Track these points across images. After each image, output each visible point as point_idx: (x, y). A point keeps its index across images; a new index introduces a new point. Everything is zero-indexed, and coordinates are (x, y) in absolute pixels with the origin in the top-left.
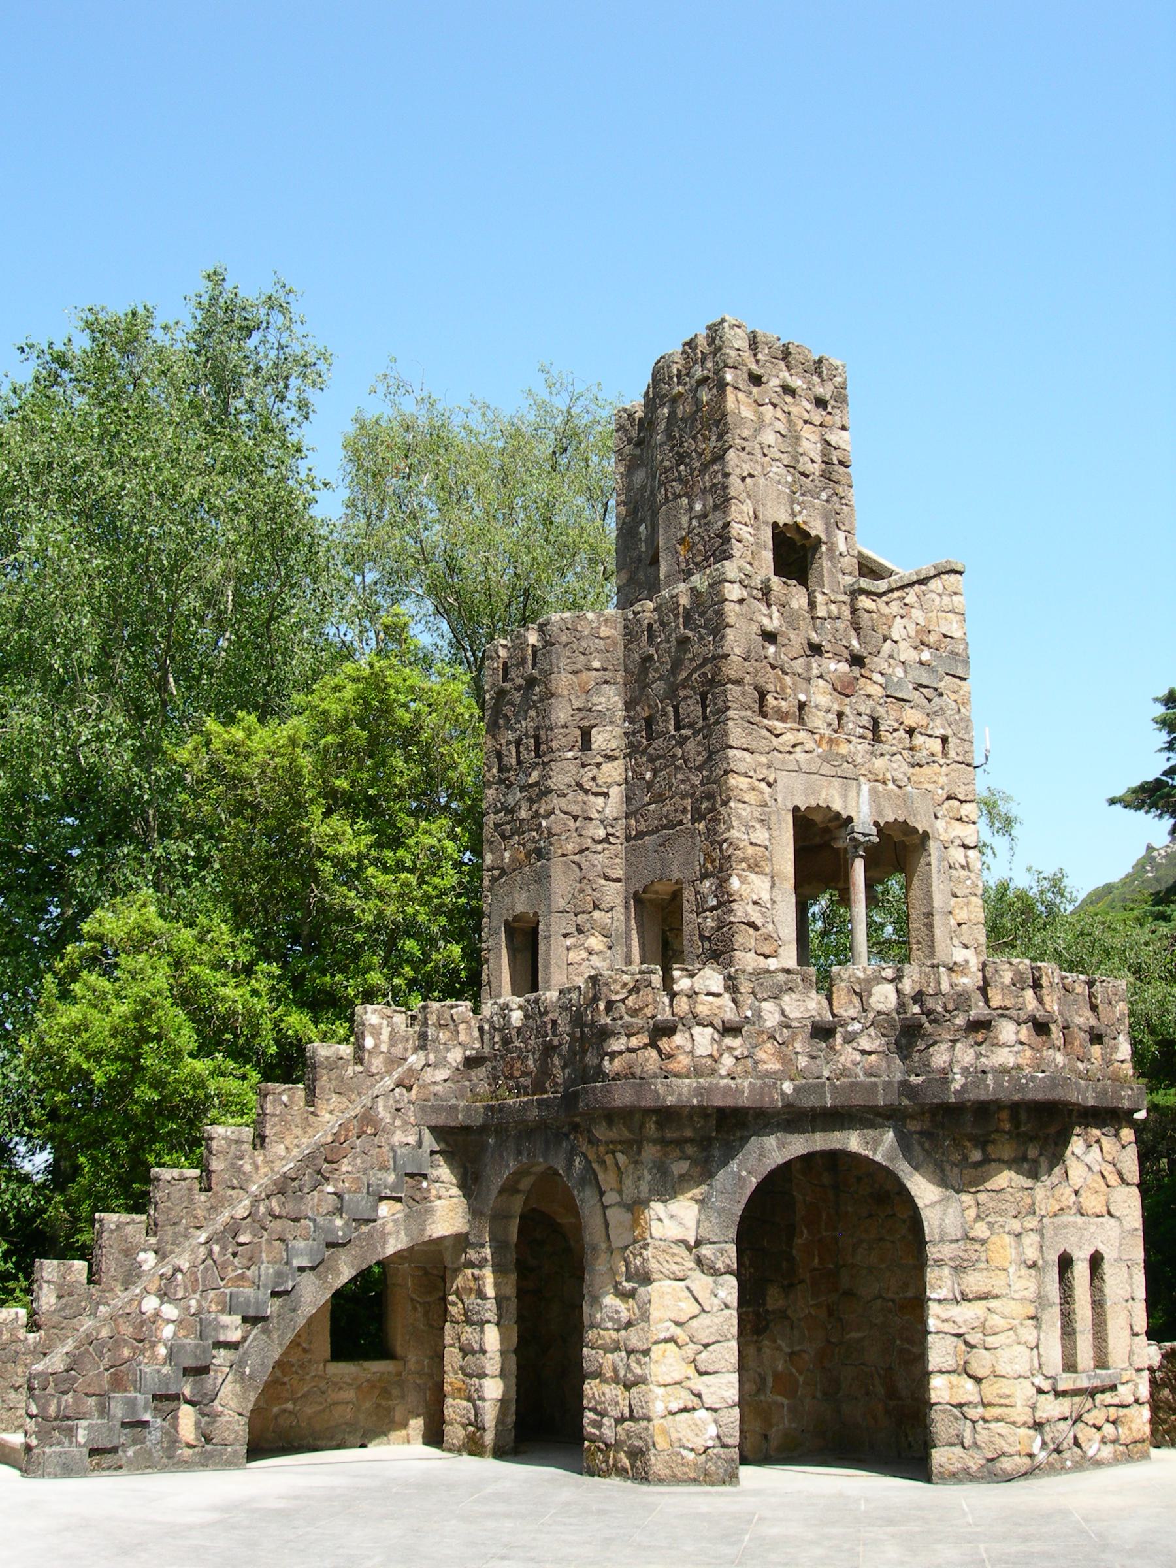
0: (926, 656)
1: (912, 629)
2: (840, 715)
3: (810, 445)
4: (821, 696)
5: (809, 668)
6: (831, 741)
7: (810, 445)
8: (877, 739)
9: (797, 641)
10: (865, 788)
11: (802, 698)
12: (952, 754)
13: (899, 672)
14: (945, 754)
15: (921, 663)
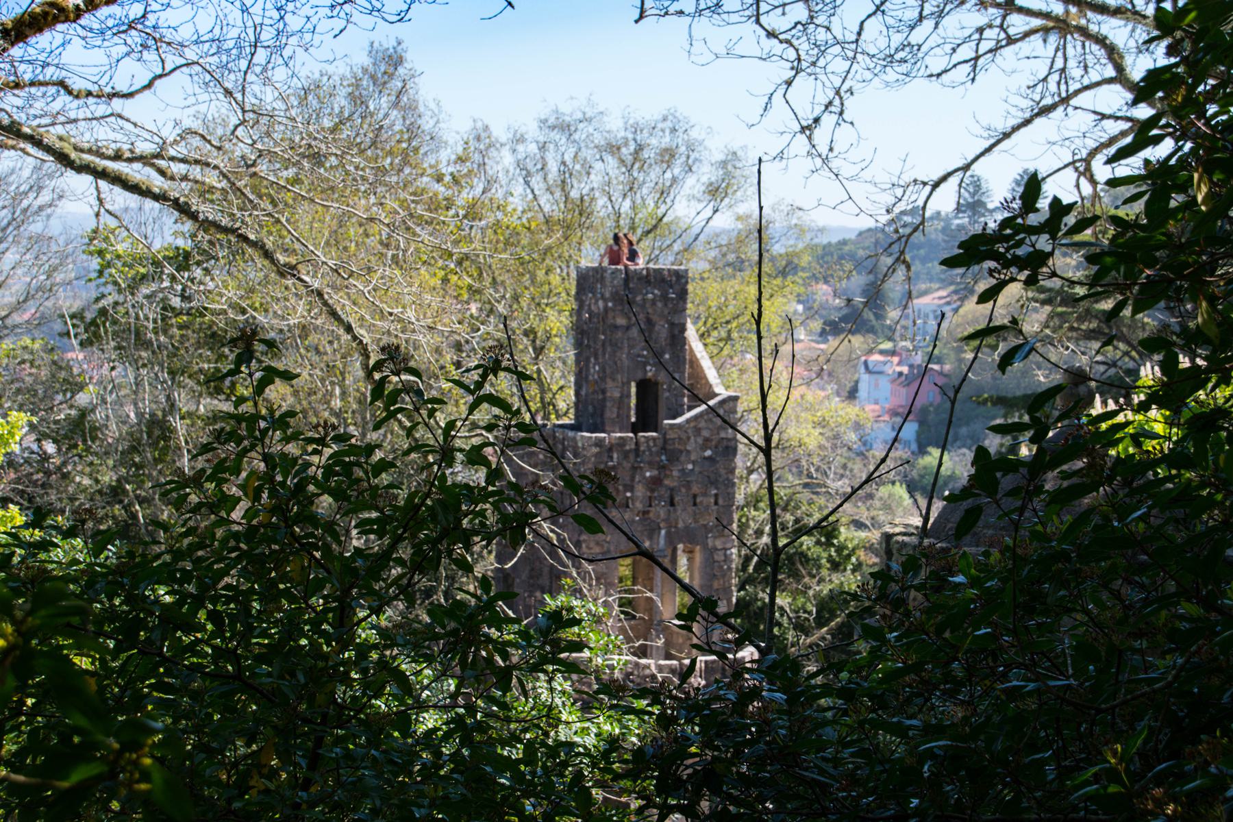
0: (708, 453)
1: (700, 440)
2: (650, 498)
3: (662, 330)
4: (640, 491)
5: (633, 479)
6: (645, 513)
7: (662, 330)
8: (672, 504)
9: (627, 465)
10: (663, 532)
11: (628, 494)
12: (721, 502)
13: (690, 467)
14: (716, 503)
15: (705, 458)
